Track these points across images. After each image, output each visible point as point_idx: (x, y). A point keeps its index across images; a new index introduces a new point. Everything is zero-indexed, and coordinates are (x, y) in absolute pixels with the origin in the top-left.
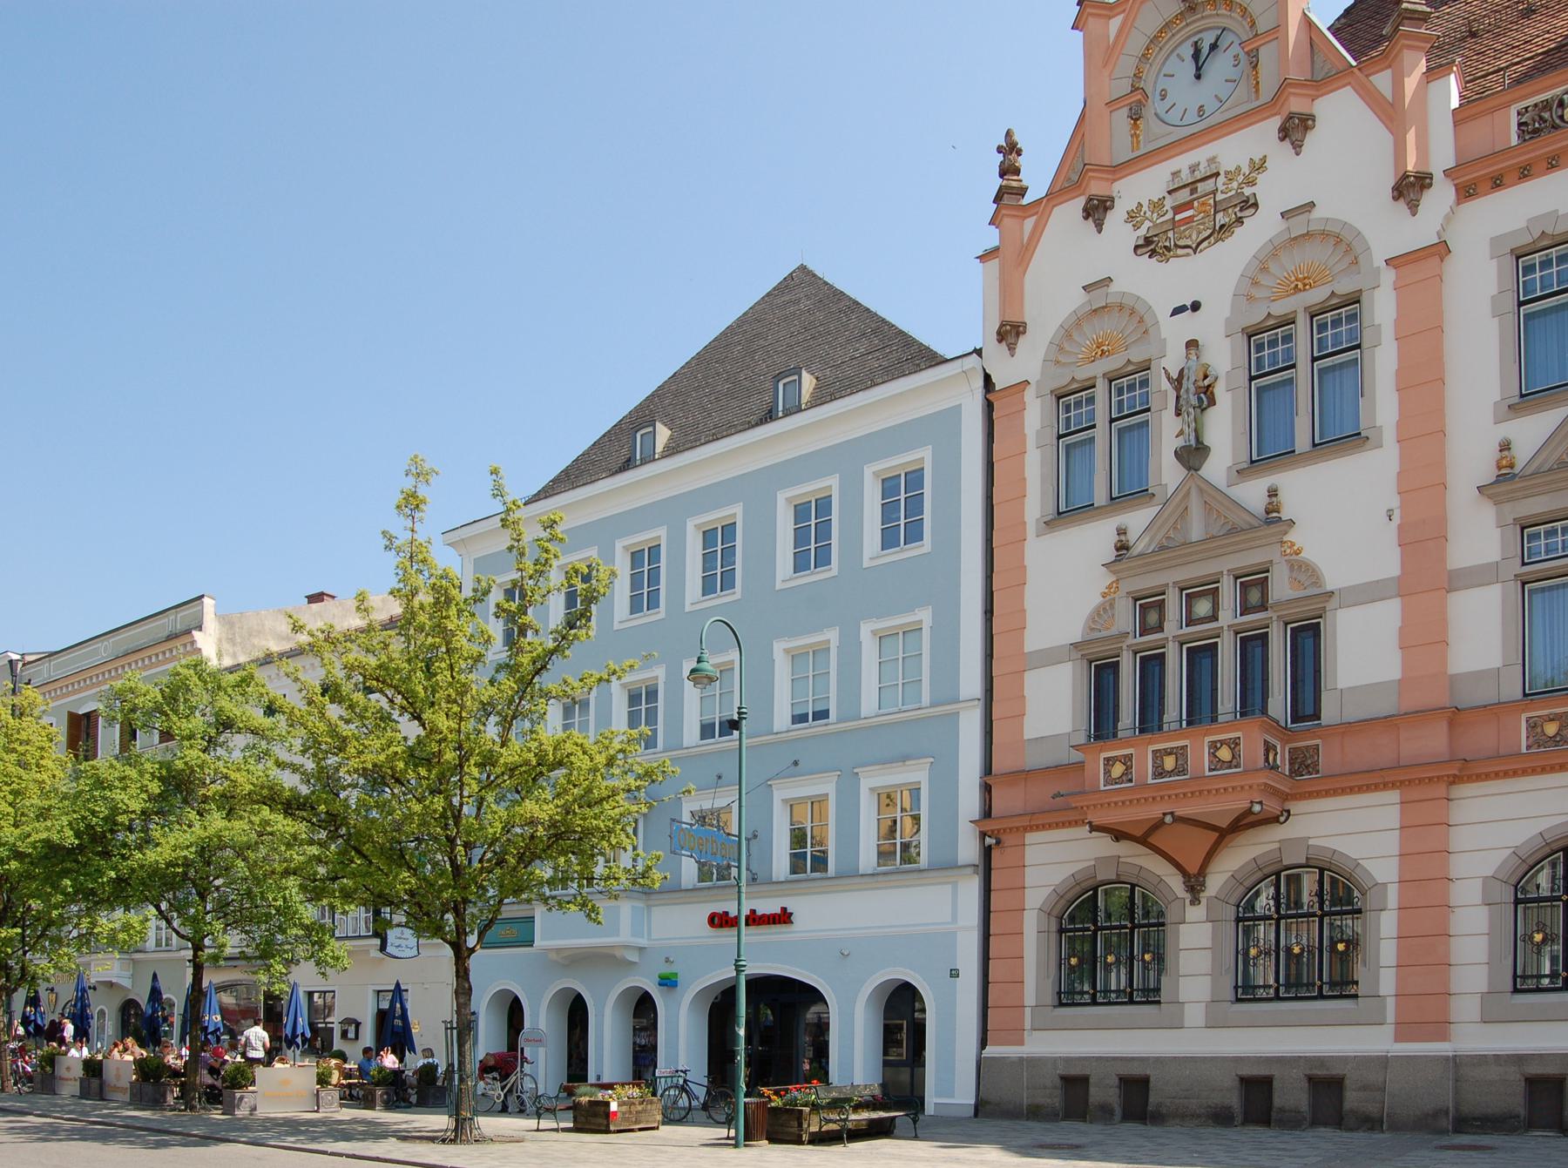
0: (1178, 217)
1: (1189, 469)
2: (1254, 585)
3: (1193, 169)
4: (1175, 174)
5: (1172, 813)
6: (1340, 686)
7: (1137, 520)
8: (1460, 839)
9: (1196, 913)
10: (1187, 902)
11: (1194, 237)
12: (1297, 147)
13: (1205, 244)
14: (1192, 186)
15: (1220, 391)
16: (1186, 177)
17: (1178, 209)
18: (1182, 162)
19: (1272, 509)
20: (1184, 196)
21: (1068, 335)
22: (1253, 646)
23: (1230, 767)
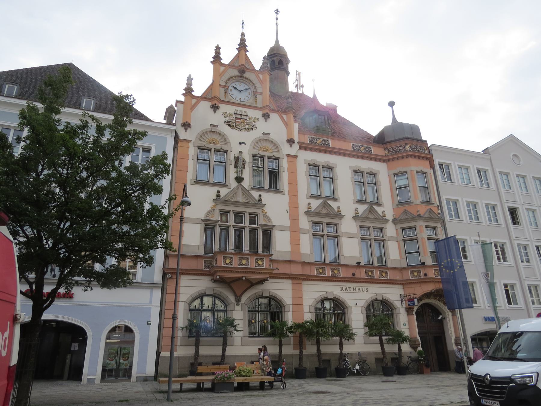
0: (237, 120)
1: (238, 183)
2: (253, 219)
3: (241, 111)
4: (236, 110)
5: (245, 277)
6: (277, 250)
7: (224, 192)
8: (305, 295)
9: (238, 308)
10: (236, 304)
11: (241, 127)
12: (266, 120)
13: (243, 130)
14: (241, 115)
15: (246, 166)
16: (238, 112)
17: (236, 118)
18: (239, 109)
19: (260, 200)
20: (238, 116)
21: (203, 134)
22: (253, 233)
23: (261, 266)
